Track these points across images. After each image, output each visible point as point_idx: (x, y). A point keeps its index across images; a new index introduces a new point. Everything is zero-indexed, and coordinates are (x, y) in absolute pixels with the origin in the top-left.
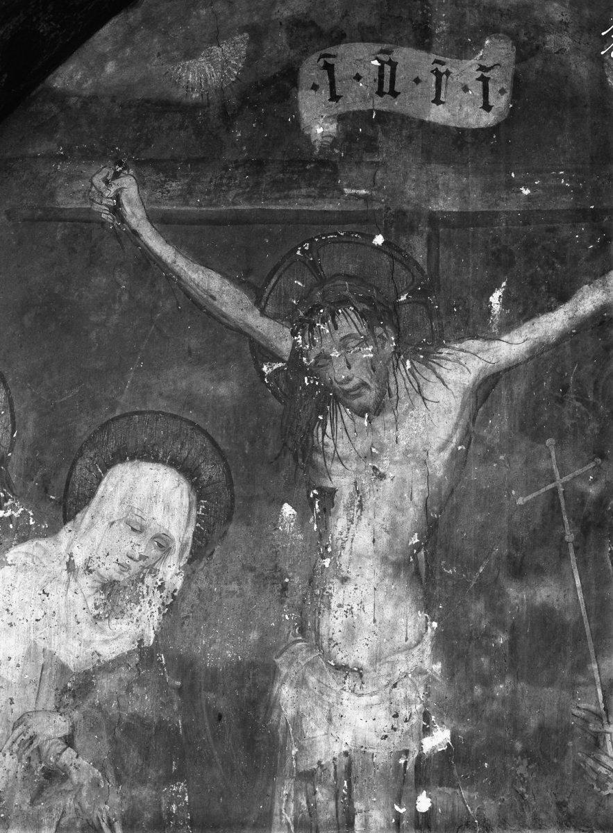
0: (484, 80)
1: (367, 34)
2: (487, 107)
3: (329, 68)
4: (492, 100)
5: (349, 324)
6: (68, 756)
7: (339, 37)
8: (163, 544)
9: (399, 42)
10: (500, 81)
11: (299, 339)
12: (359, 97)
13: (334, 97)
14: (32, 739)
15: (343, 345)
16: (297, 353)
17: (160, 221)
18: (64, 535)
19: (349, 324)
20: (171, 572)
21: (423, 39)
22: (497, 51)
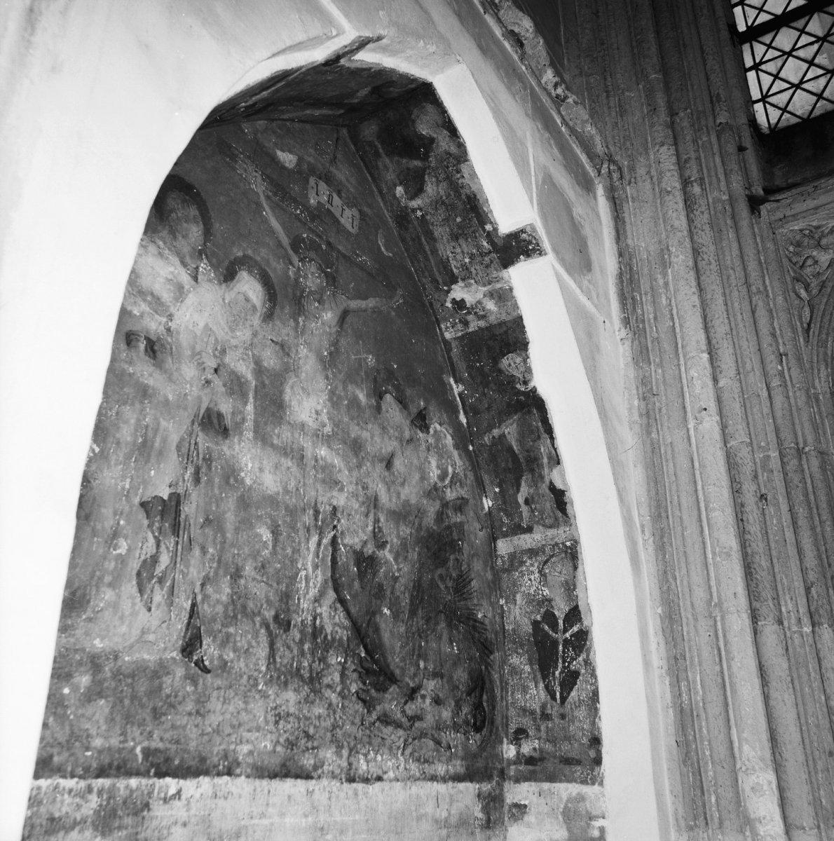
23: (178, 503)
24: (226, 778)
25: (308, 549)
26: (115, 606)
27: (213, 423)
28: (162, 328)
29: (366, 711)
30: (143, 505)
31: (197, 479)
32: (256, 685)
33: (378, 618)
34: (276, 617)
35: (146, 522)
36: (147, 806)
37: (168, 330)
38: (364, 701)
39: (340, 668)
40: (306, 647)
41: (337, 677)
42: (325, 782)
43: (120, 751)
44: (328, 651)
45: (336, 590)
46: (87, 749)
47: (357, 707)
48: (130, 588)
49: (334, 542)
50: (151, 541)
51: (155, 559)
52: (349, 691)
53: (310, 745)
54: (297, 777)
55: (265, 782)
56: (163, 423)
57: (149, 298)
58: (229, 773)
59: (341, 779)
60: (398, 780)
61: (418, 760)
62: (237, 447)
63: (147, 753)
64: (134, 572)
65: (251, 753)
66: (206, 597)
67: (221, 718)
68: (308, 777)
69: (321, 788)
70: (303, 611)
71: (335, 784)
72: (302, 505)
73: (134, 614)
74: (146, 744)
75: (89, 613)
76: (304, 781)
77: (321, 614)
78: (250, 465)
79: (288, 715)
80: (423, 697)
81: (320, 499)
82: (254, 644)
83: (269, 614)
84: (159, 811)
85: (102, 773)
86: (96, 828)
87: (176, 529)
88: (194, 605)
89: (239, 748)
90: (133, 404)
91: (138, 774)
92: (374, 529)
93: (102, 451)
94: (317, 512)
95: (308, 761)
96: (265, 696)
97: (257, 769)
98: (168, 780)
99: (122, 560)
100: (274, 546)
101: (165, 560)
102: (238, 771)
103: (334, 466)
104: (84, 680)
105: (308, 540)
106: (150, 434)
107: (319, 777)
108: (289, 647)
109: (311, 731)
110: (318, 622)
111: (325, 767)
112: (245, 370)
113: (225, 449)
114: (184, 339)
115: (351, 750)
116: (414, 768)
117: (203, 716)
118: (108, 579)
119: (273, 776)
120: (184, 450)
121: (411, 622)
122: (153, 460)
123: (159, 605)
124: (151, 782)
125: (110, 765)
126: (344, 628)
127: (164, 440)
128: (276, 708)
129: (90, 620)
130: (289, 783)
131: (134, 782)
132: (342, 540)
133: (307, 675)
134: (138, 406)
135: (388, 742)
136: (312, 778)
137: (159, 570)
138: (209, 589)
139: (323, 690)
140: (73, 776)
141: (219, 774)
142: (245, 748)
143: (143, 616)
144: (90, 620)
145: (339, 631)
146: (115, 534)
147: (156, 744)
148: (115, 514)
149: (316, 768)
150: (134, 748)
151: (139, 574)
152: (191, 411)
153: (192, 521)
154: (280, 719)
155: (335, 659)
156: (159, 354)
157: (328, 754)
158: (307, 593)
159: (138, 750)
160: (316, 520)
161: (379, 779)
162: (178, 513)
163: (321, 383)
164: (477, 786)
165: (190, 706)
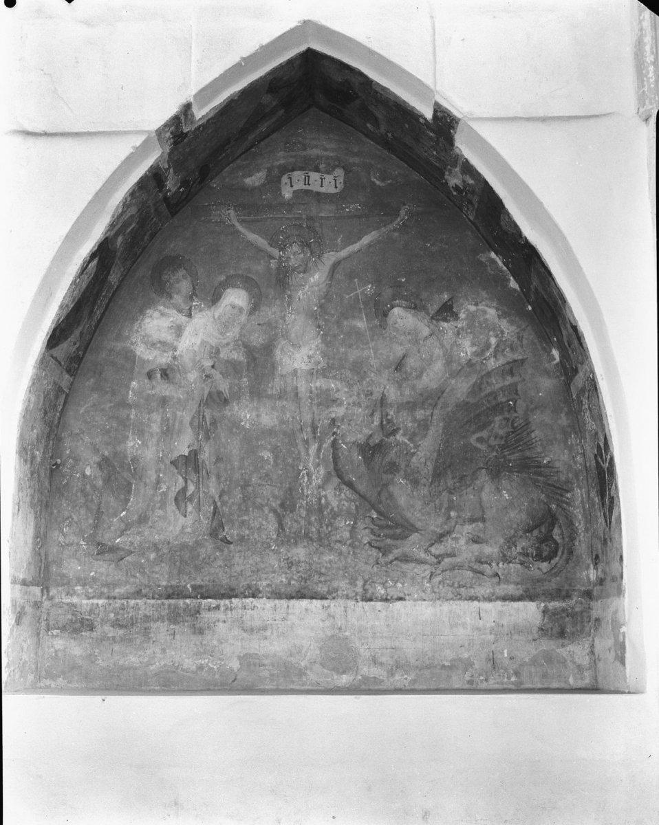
0: (335, 180)
1: (301, 169)
2: (336, 187)
3: (290, 178)
4: (337, 185)
5: (295, 248)
6: (213, 371)
7: (293, 170)
8: (241, 309)
9: (310, 170)
10: (341, 180)
11: (281, 253)
12: (300, 186)
13: (292, 186)
14: (203, 366)
15: (294, 254)
16: (280, 257)
17: (242, 222)
18: (213, 308)
19: (295, 248)
20: (243, 318)
21: (317, 170)
22: (339, 172)
23: (196, 455)
24: (251, 599)
25: (308, 455)
26: (164, 518)
27: (217, 400)
28: (170, 358)
29: (381, 554)
30: (171, 463)
31: (207, 438)
32: (270, 547)
33: (391, 488)
34: (282, 505)
35: (176, 471)
36: (198, 612)
37: (175, 358)
38: (379, 548)
39: (349, 528)
40: (313, 519)
41: (346, 535)
42: (341, 602)
43: (178, 587)
44: (335, 519)
45: (340, 477)
46: (159, 586)
47: (370, 553)
48: (172, 507)
49: (334, 444)
50: (181, 480)
51: (185, 489)
52: (360, 542)
53: (323, 579)
54: (312, 598)
55: (284, 602)
56: (179, 414)
57: (159, 345)
58: (254, 596)
59: (356, 599)
60: (424, 600)
61: (452, 586)
62: (236, 408)
63: (194, 587)
64: (173, 499)
65: (269, 585)
66: (224, 503)
67: (243, 567)
68: (323, 598)
69: (336, 606)
70: (307, 497)
71: (351, 603)
72: (299, 427)
73: (176, 520)
74: (193, 583)
75: (150, 523)
76: (319, 601)
77: (326, 497)
78: (248, 416)
79: (299, 562)
80: (456, 539)
81: (317, 418)
82: (264, 523)
83: (275, 504)
84: (206, 615)
85: (169, 597)
86: (169, 620)
87: (197, 470)
88: (216, 508)
89: (259, 583)
90: (157, 411)
91: (190, 597)
92: (382, 422)
93: (143, 443)
94: (314, 429)
95: (322, 589)
96: (276, 552)
97: (276, 594)
98: (210, 600)
99: (165, 494)
100: (275, 461)
101: (191, 488)
102: (260, 595)
103: (328, 390)
104: (152, 556)
105: (307, 450)
106: (171, 422)
107: (334, 598)
108: (296, 521)
109: (323, 570)
110: (323, 501)
111: (340, 592)
112: (238, 356)
113: (226, 412)
114: (187, 360)
115: (366, 582)
116: (443, 590)
117: (230, 567)
118: (159, 505)
119: (290, 597)
120: (196, 424)
121: (436, 484)
122: (175, 436)
123: (191, 512)
124: (199, 601)
125: (173, 594)
126: (354, 501)
127: (181, 422)
128: (288, 559)
129: (151, 527)
130: (304, 603)
131: (188, 601)
132: (343, 440)
133: (315, 537)
134: (161, 410)
135: (410, 574)
136: (327, 599)
137: (189, 493)
138: (226, 498)
139: (332, 545)
140: (153, 598)
141: (245, 597)
142: (264, 583)
143: (182, 520)
144: (151, 527)
145: (346, 504)
146: (158, 481)
147: (199, 582)
148: (156, 472)
149: (329, 592)
150: (186, 585)
151: (176, 499)
152: (197, 399)
153: (207, 463)
154: (292, 564)
155: (343, 524)
156: (171, 376)
157: (343, 584)
158: (311, 484)
159: (188, 586)
160: (314, 432)
161: (401, 599)
162: (196, 460)
163: (312, 331)
164: (543, 605)
165: (220, 563)
